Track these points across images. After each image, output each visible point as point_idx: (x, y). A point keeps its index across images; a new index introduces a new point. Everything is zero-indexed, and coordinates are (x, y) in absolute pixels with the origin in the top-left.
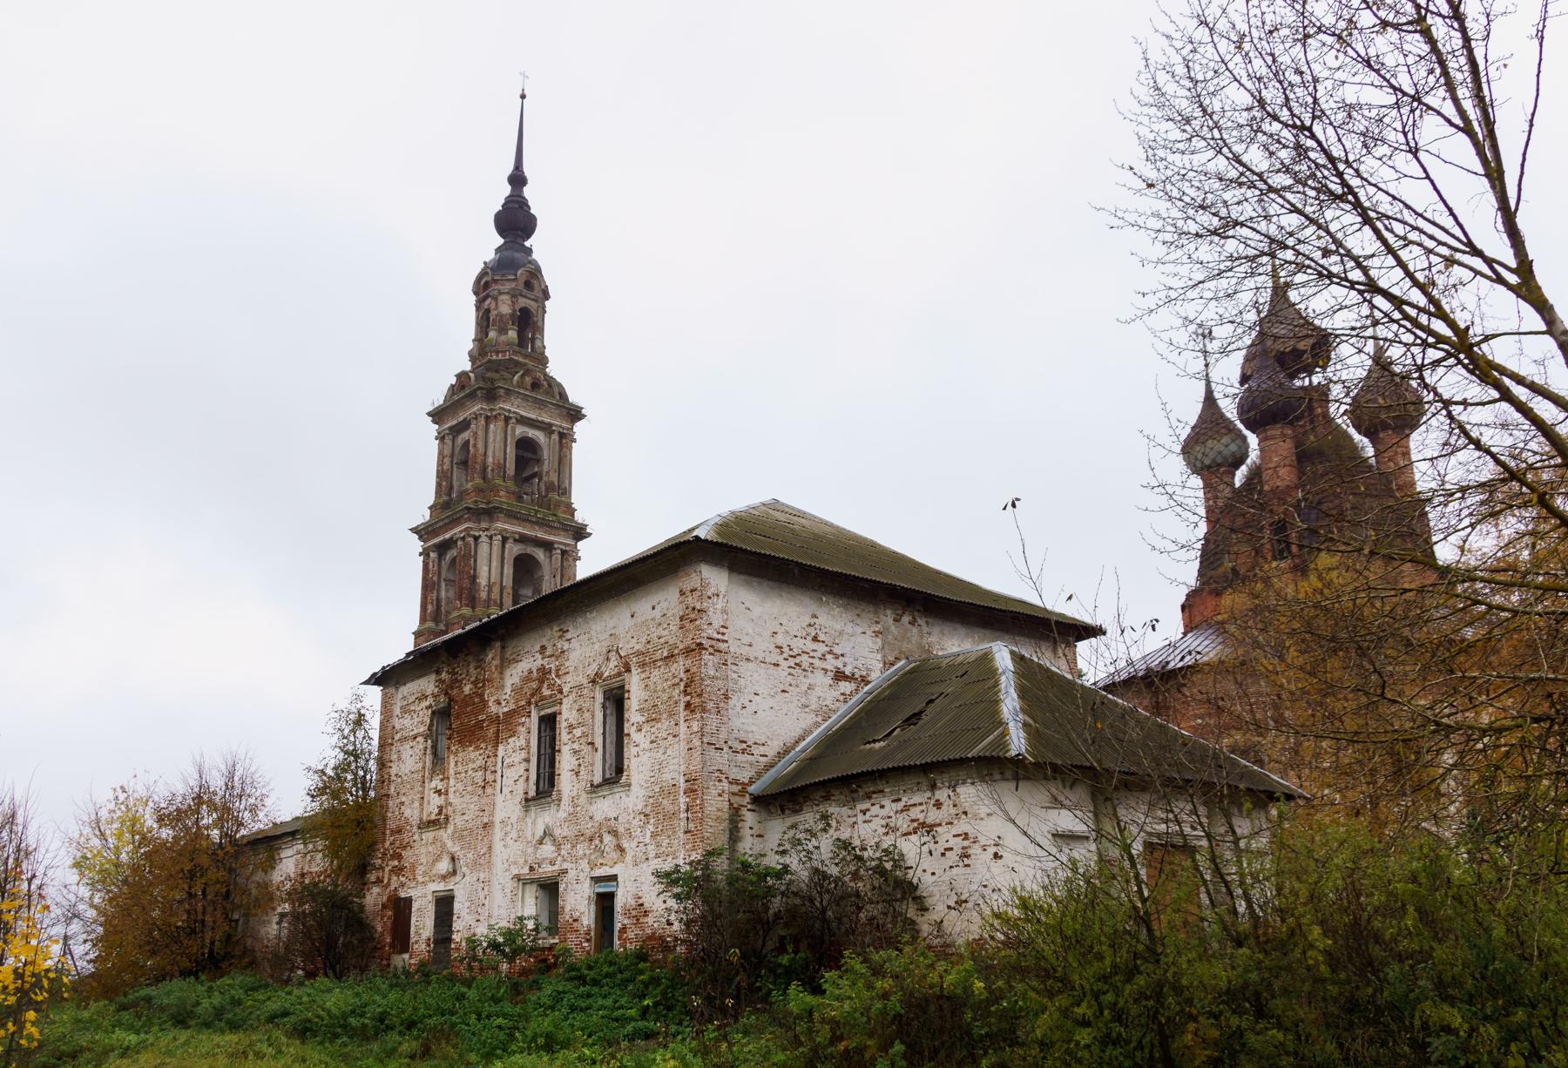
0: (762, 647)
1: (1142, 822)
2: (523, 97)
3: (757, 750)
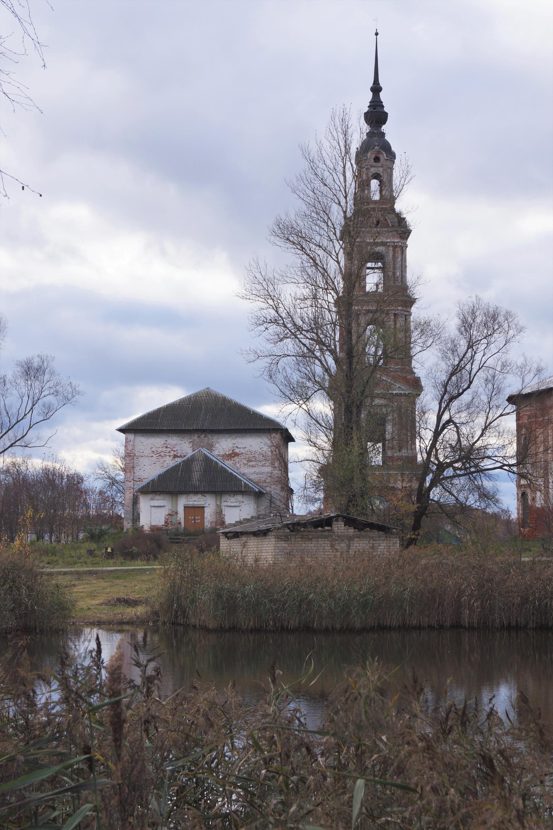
0: (147, 452)
1: (183, 502)
2: (377, 34)
3: (144, 480)
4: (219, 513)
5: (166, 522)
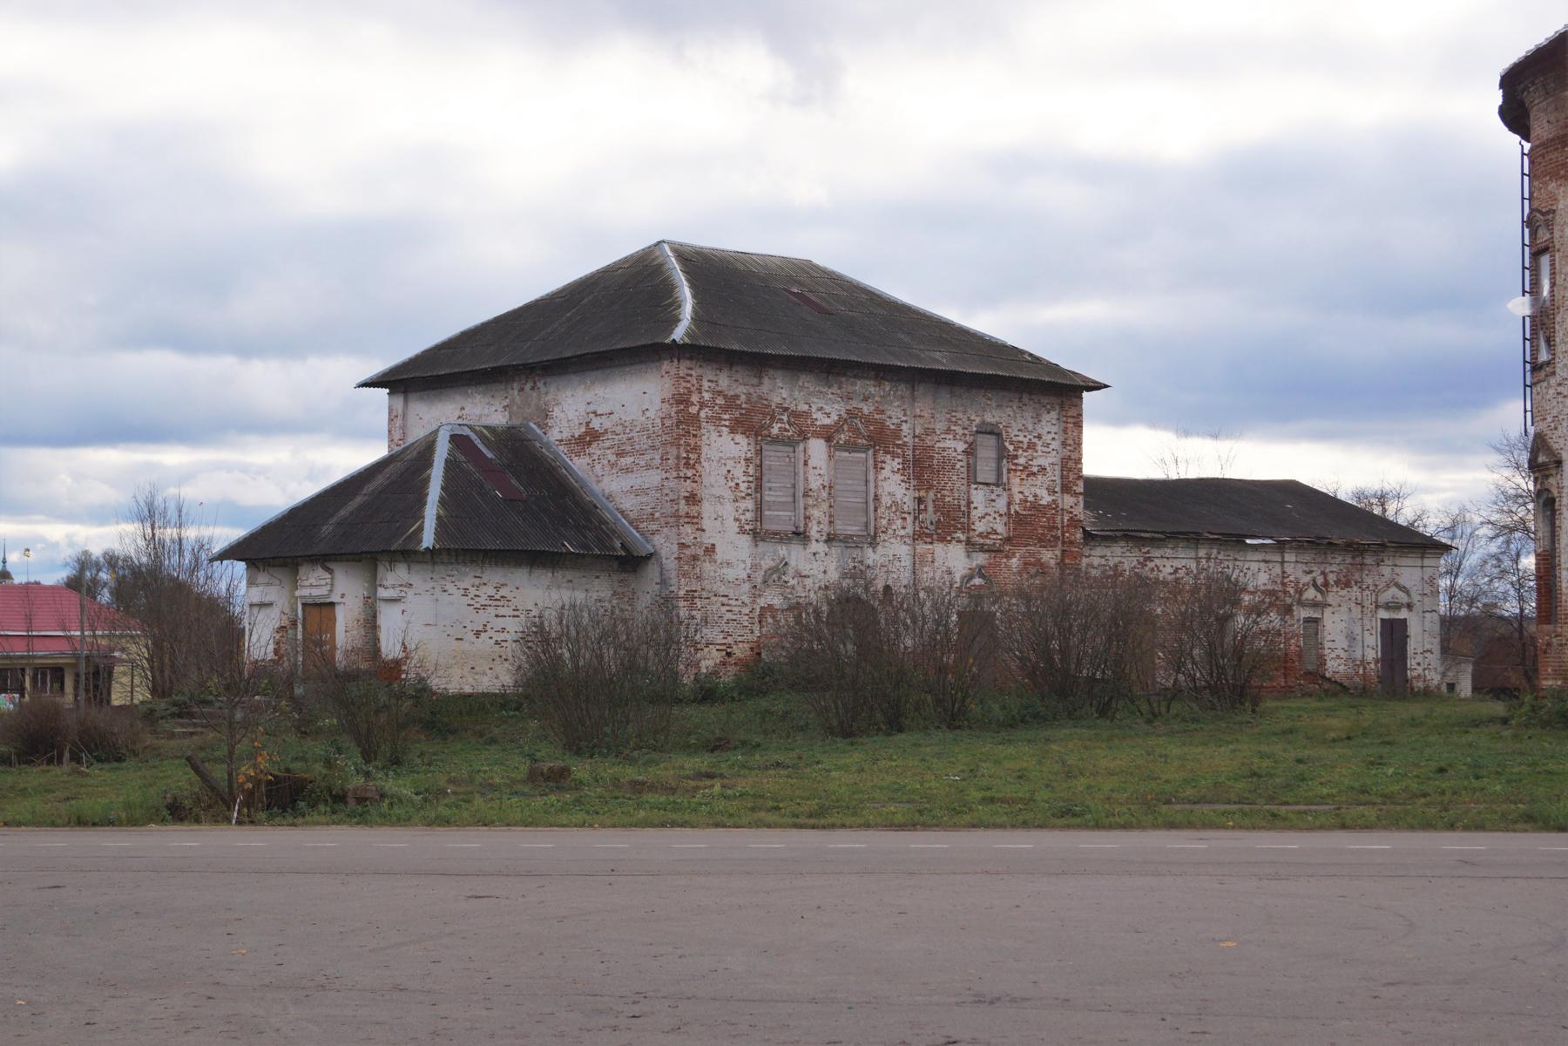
4: (371, 624)
5: (276, 652)
